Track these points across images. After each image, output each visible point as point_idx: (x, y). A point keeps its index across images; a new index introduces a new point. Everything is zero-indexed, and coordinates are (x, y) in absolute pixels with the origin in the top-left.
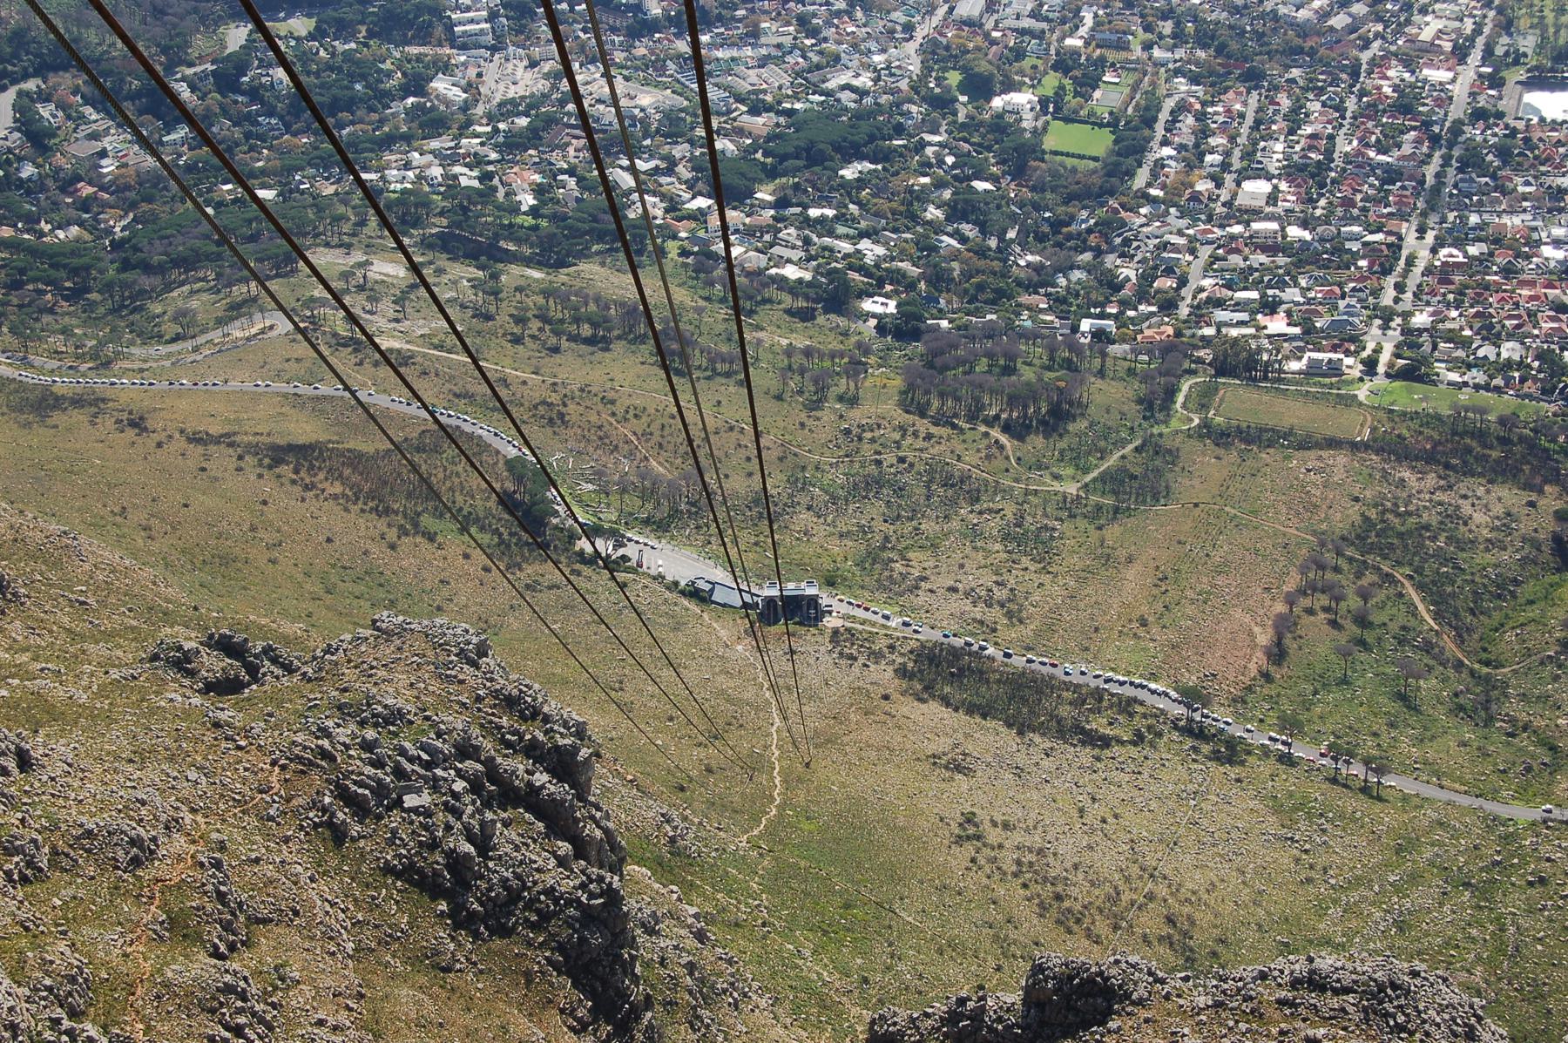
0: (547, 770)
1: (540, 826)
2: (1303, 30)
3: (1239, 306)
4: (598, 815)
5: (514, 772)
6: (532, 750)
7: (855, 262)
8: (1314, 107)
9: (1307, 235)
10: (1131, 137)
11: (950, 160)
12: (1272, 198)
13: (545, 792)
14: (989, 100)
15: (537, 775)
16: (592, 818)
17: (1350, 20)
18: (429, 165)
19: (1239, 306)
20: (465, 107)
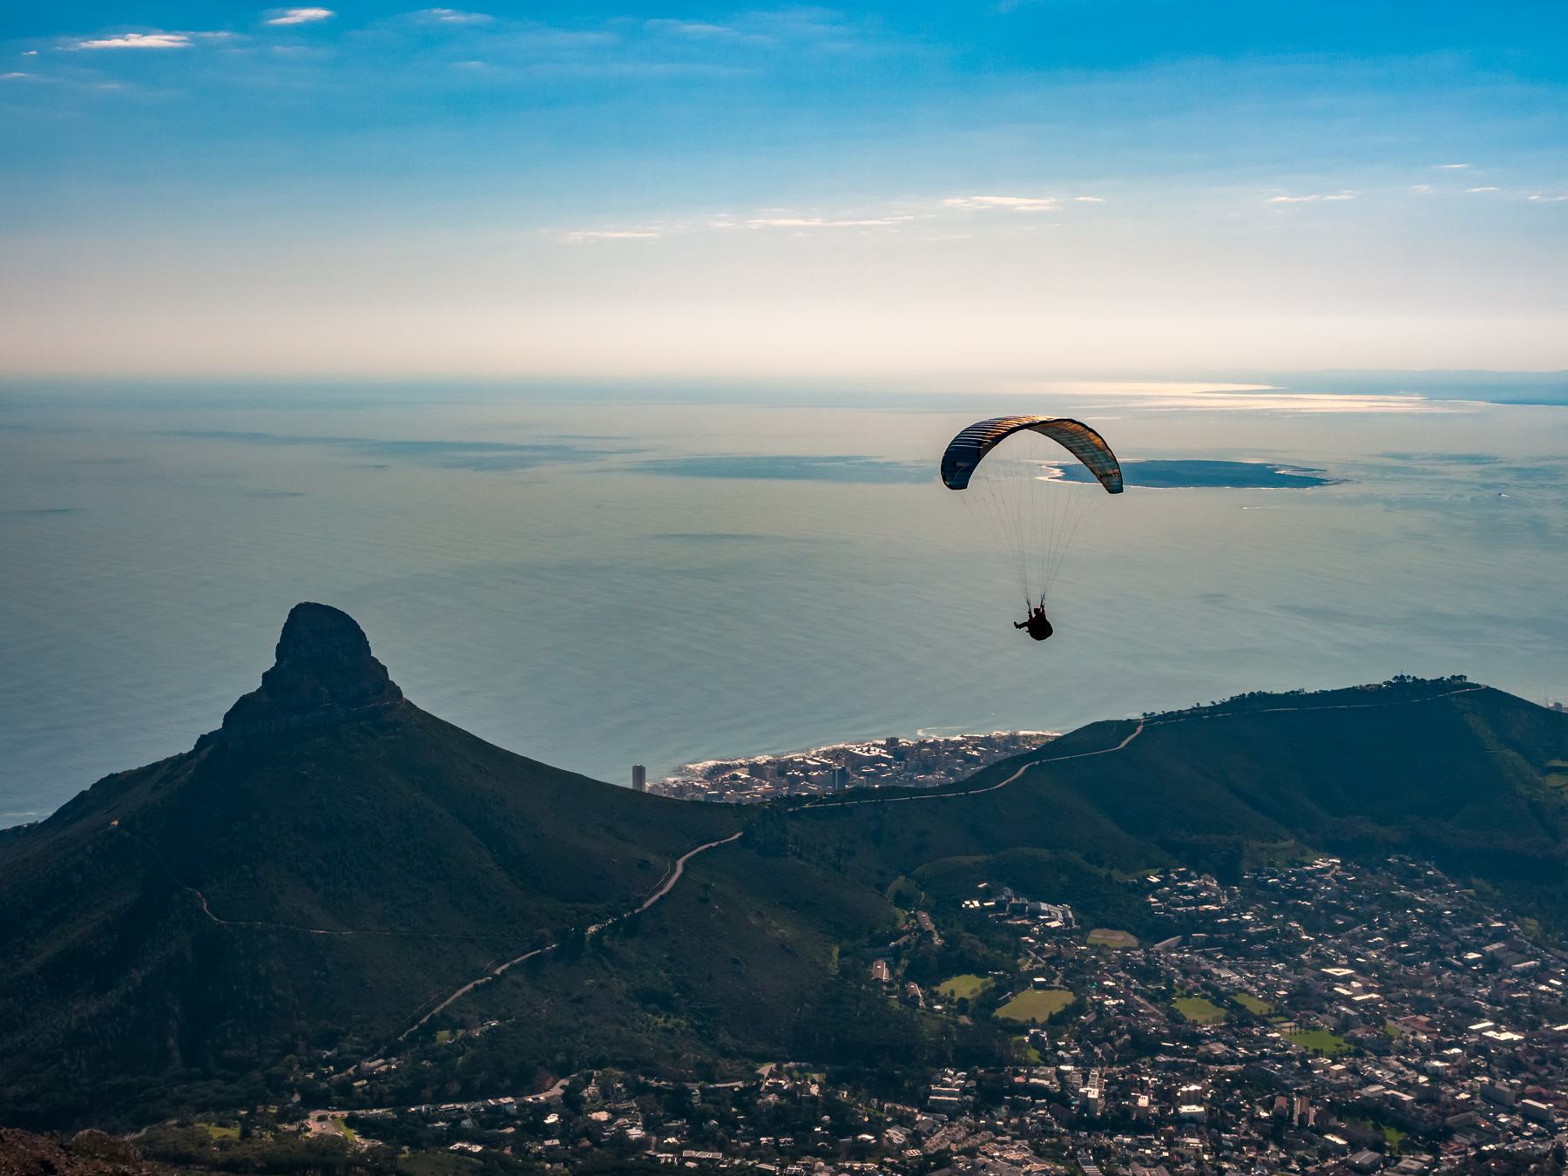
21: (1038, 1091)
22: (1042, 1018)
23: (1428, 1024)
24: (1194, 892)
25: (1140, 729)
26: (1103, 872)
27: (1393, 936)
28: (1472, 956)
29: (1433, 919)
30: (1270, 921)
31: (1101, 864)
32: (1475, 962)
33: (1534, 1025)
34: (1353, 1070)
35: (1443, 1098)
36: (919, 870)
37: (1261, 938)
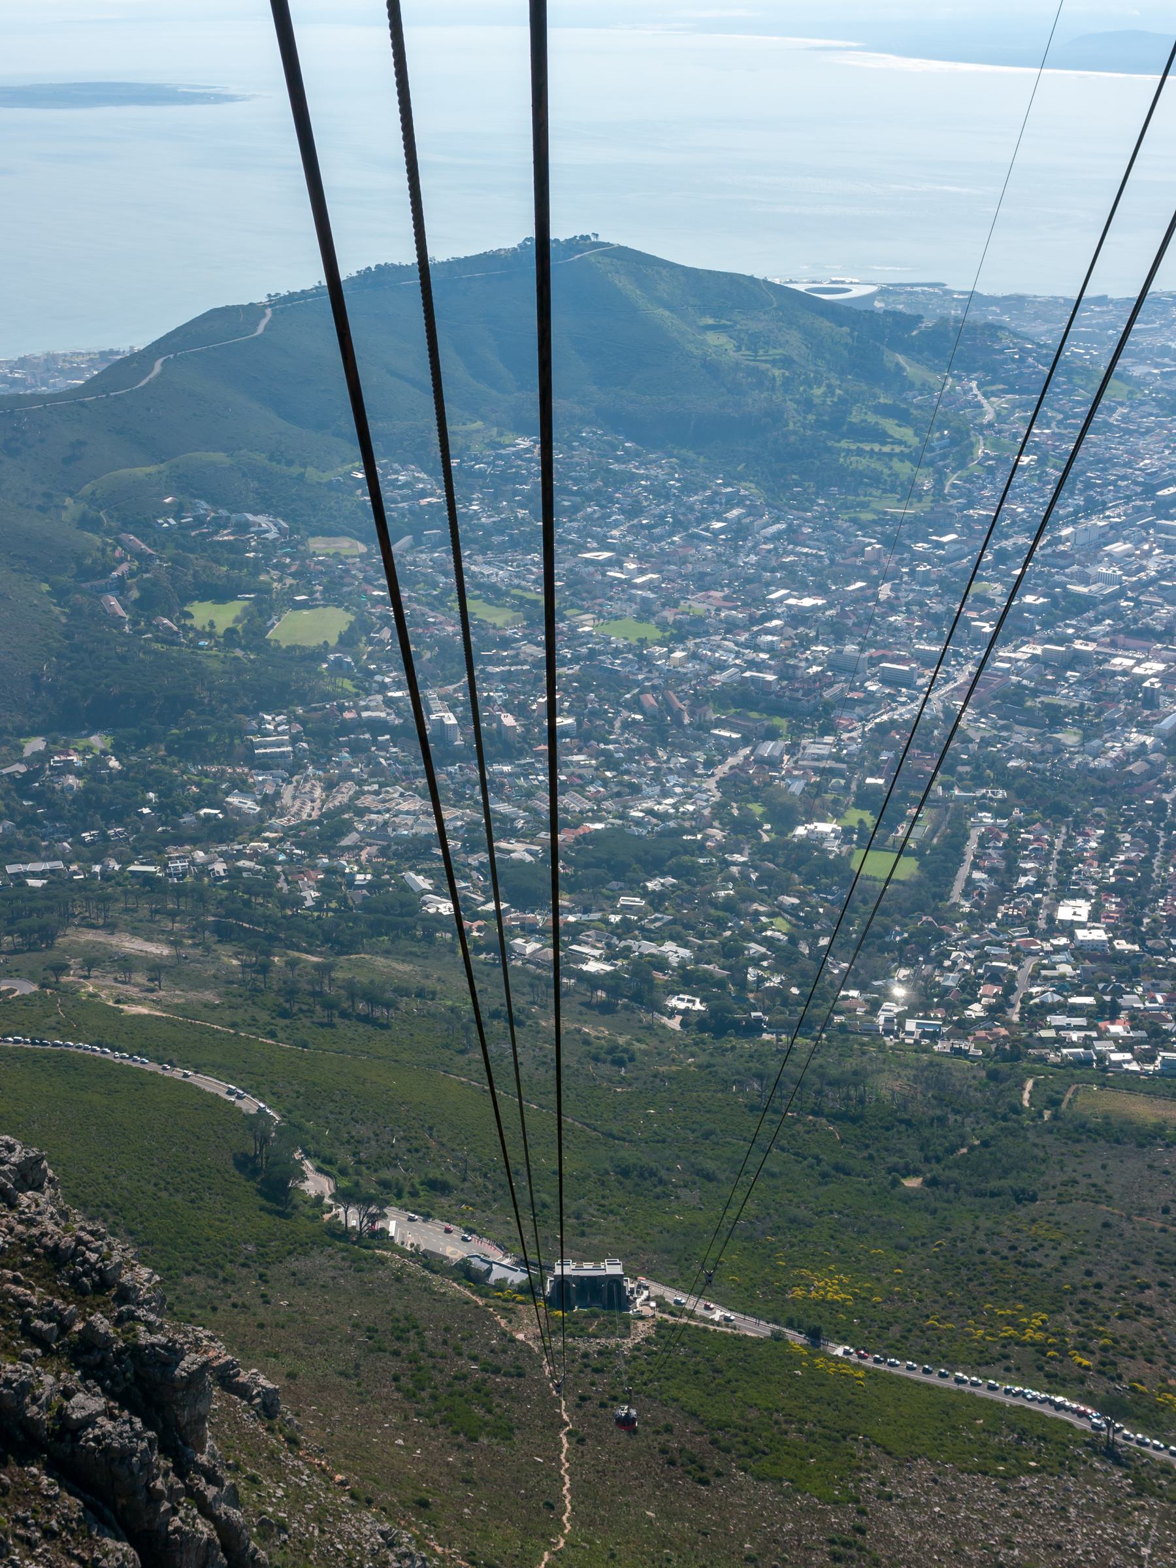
0: (108, 1393)
1: (72, 1504)
2: (1101, 774)
3: (1074, 1011)
4: (211, 1492)
5: (25, 1388)
6: (89, 1358)
7: (660, 963)
8: (1126, 837)
9: (1136, 948)
10: (941, 862)
11: (753, 877)
12: (1095, 916)
13: (91, 1433)
14: (792, 829)
15: (79, 1398)
16: (198, 1498)
17: (1147, 766)
18: (212, 862)
19: (1074, 1011)
20: (260, 818)
21: (377, 727)
22: (333, 641)
23: (725, 598)
24: (406, 485)
25: (269, 311)
26: (295, 470)
27: (633, 511)
28: (718, 525)
29: (660, 492)
30: (499, 511)
31: (290, 463)
32: (722, 531)
33: (820, 590)
34: (694, 656)
35: (799, 673)
36: (88, 488)
37: (499, 528)
